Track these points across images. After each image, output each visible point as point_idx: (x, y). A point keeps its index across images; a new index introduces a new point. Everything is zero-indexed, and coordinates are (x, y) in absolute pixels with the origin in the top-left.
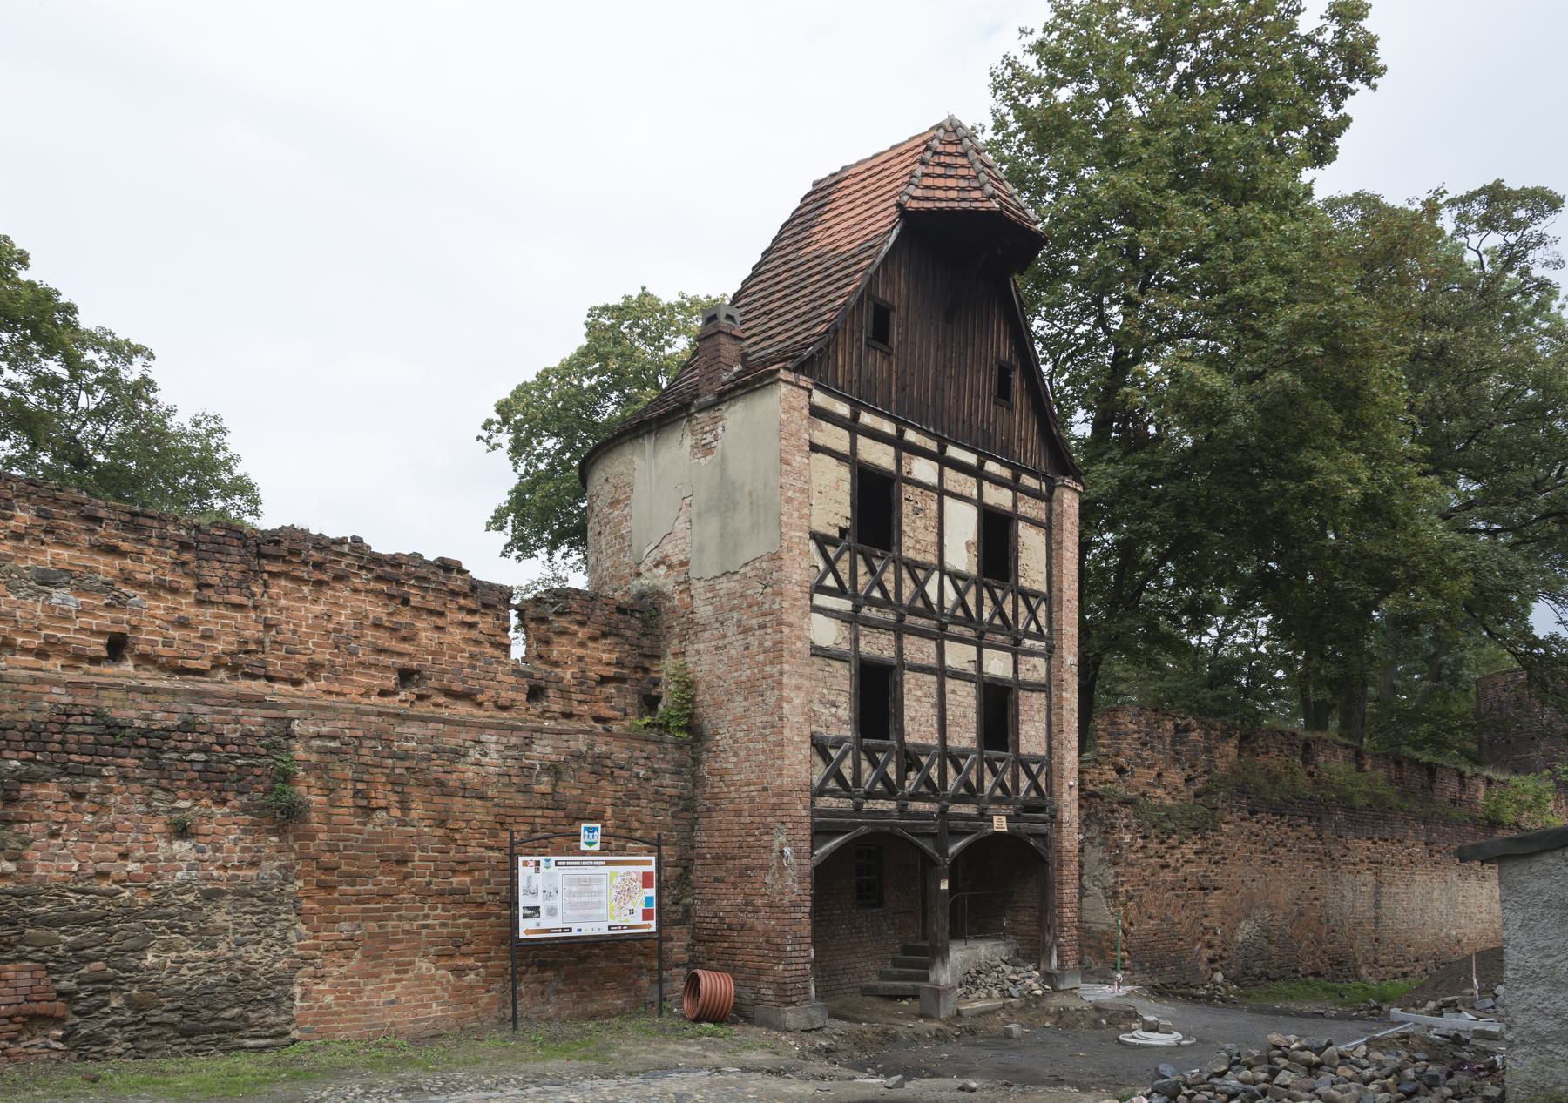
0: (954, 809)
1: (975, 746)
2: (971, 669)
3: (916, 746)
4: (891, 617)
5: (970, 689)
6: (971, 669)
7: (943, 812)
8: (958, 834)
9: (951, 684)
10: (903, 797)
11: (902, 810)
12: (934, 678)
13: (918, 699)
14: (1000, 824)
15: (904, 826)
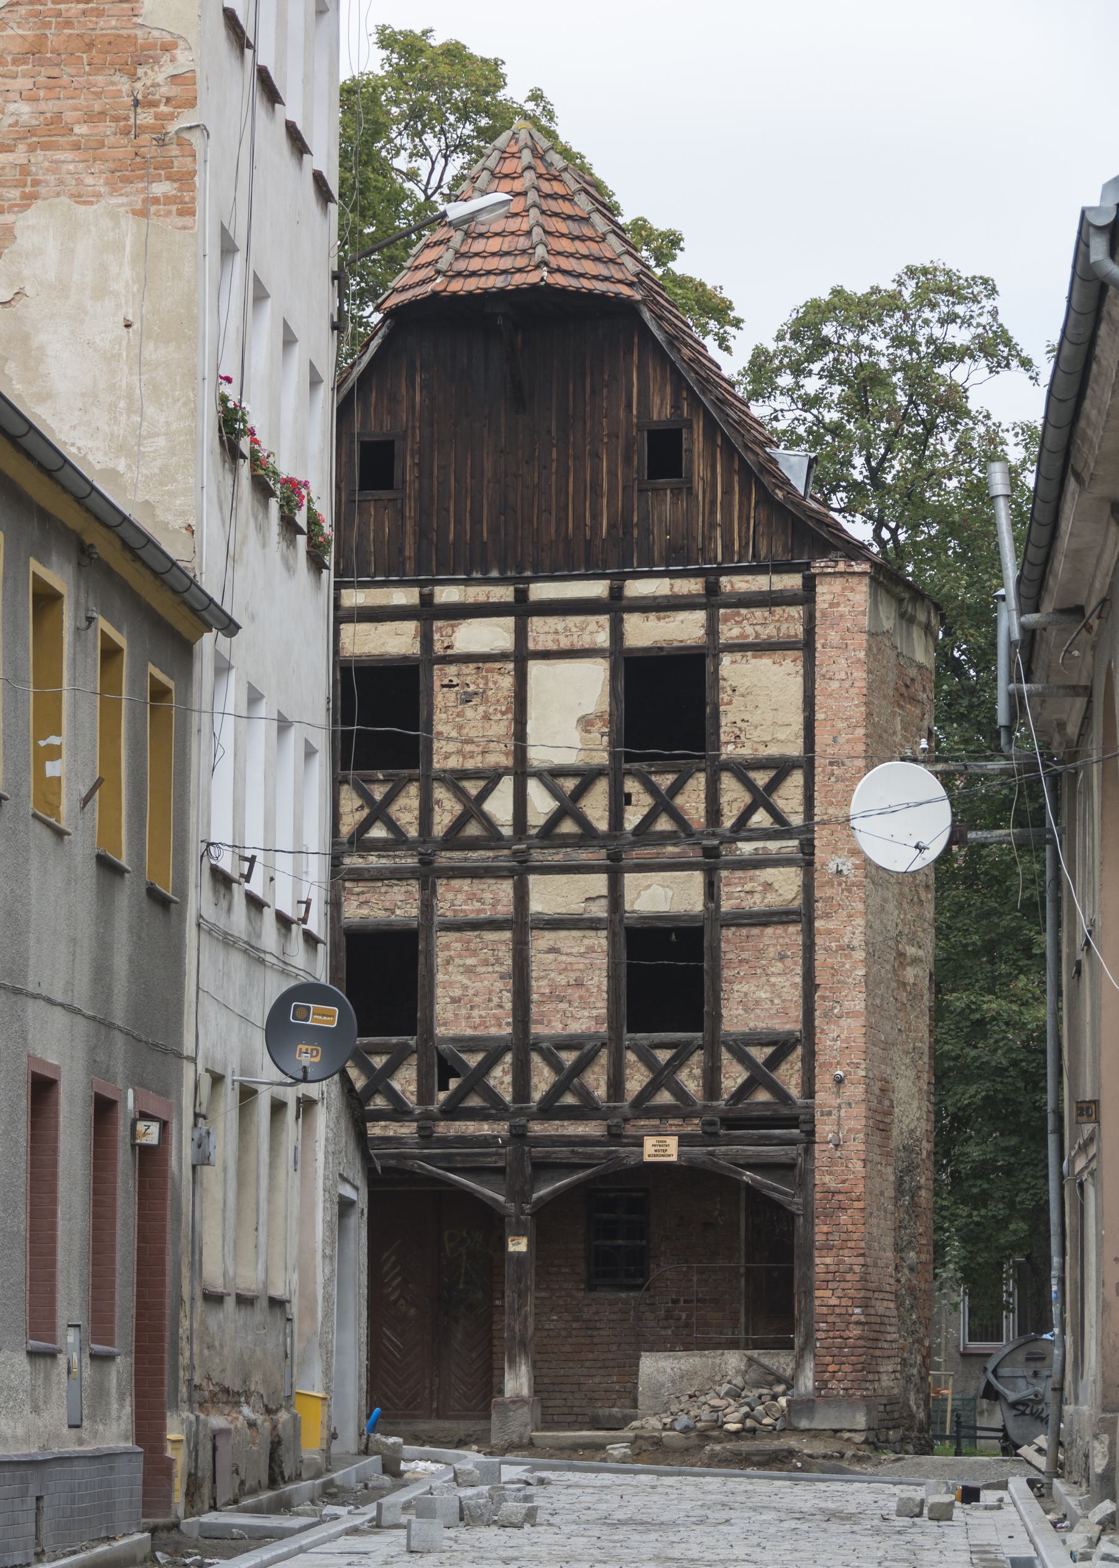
0: (538, 1128)
1: (603, 1028)
2: (599, 910)
3: (455, 1040)
4: (411, 861)
5: (600, 940)
6: (599, 910)
7: (519, 1135)
8: (545, 1168)
9: (541, 941)
10: (427, 1116)
11: (426, 1136)
12: (507, 935)
13: (469, 970)
14: (661, 1148)
15: (428, 1159)
